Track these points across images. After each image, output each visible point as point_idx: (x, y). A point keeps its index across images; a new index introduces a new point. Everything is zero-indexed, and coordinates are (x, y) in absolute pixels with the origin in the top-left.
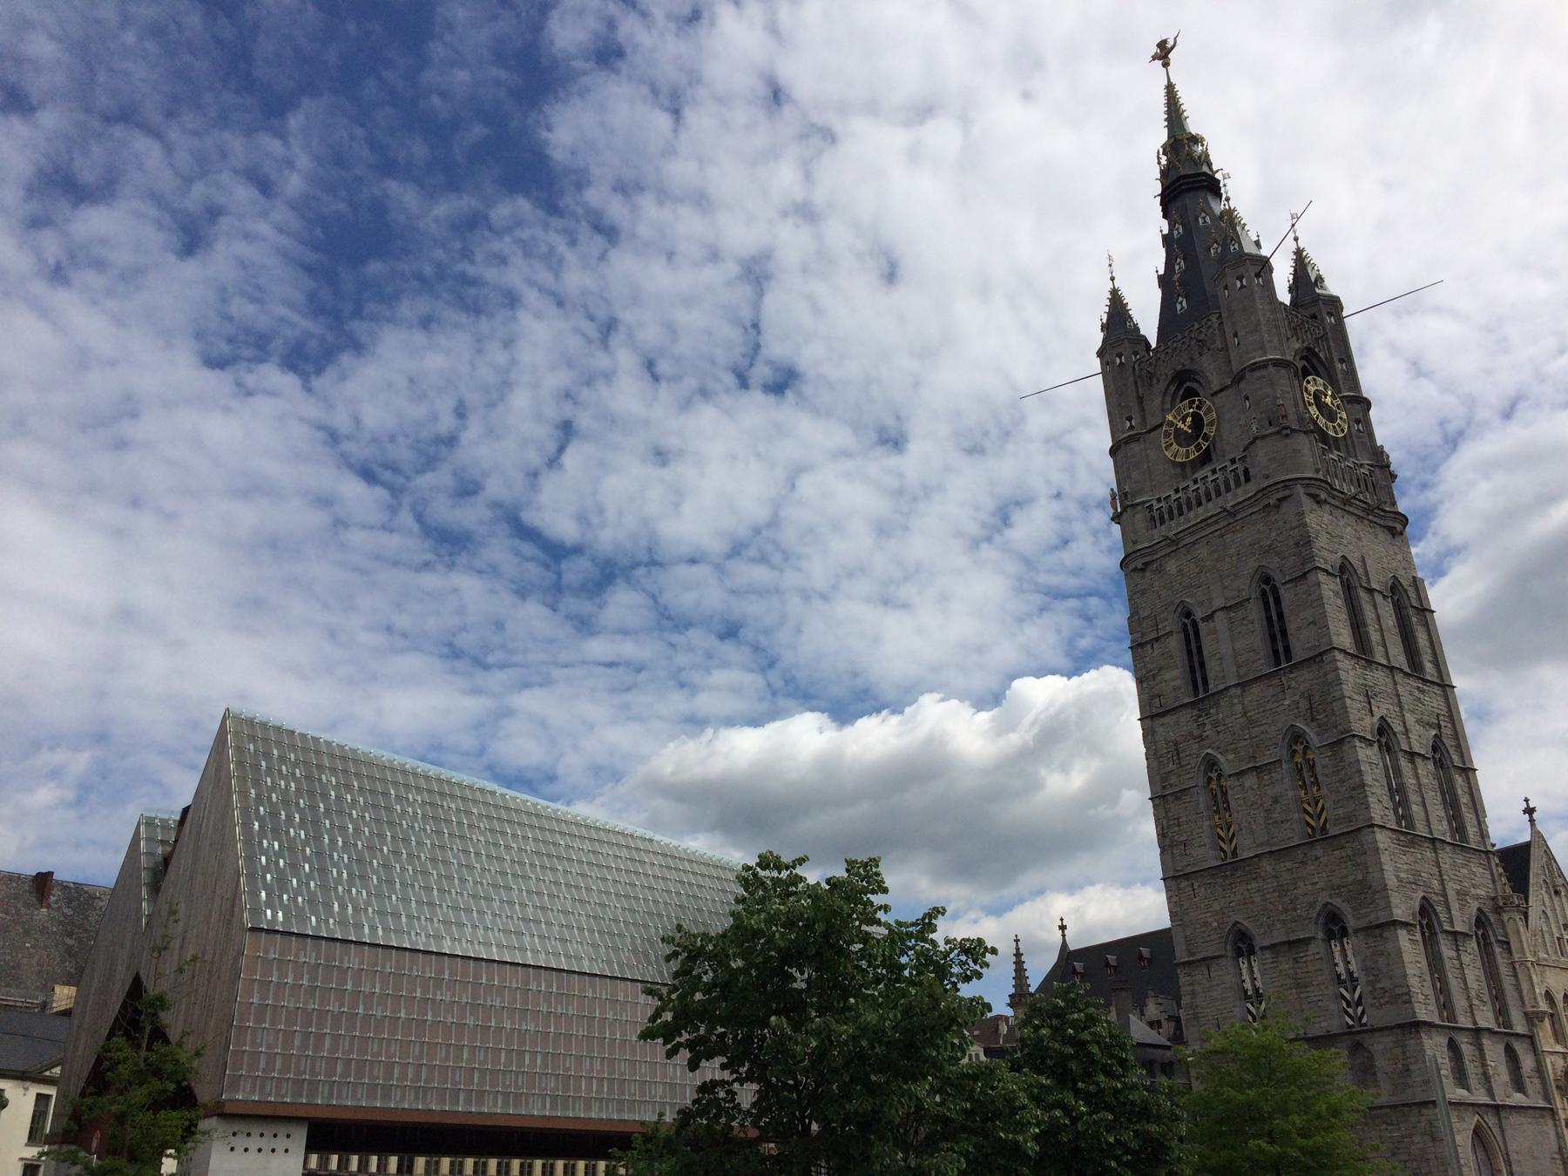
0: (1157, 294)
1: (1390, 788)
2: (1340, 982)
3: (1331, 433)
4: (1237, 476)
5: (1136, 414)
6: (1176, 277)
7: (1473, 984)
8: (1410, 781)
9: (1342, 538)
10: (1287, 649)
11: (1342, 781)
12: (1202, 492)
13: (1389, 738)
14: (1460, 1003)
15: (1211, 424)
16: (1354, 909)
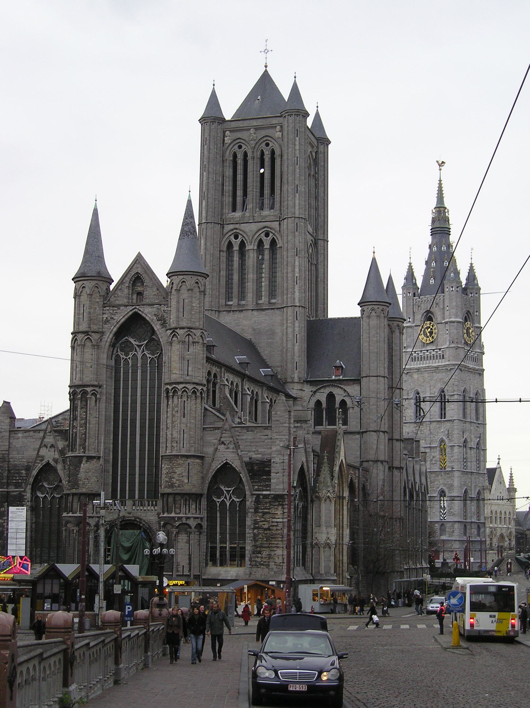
0: (424, 267)
1: (464, 457)
2: (441, 507)
3: (469, 342)
4: (440, 356)
5: (411, 318)
6: (432, 270)
7: (473, 510)
8: (469, 456)
9: (466, 380)
10: (445, 414)
11: (452, 456)
12: (429, 356)
13: (466, 444)
14: (469, 515)
15: (435, 333)
16: (448, 491)
